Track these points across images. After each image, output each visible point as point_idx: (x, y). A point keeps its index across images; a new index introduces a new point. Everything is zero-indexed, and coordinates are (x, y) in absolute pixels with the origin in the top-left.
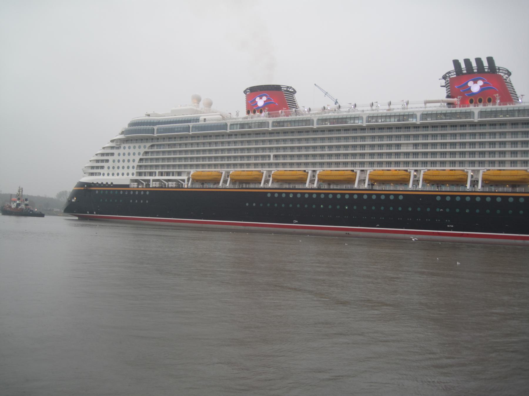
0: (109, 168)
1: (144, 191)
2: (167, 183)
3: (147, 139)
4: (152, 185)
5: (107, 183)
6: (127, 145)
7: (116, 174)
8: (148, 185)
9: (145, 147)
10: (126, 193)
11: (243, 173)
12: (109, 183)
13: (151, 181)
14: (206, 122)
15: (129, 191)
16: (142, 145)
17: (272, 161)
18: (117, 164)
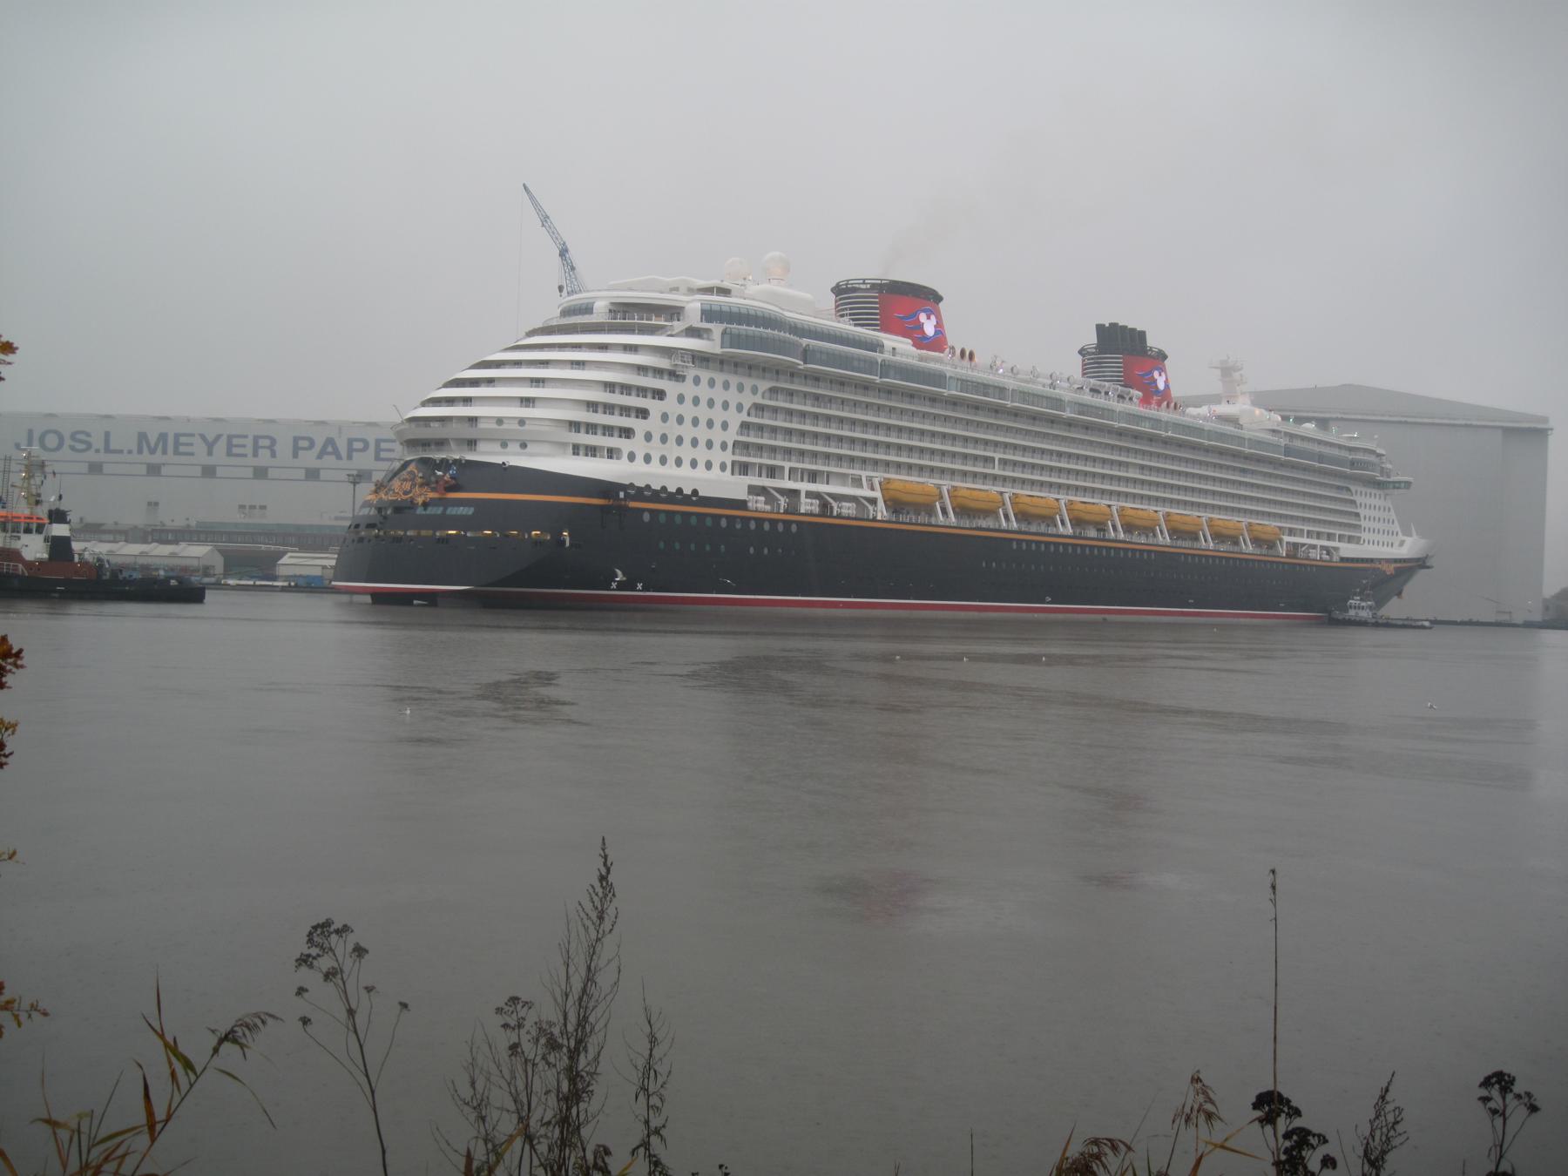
0: (648, 437)
1: (784, 522)
2: (835, 505)
3: (764, 369)
4: (806, 505)
5: (680, 490)
6: (705, 375)
7: (671, 461)
8: (792, 509)
9: (754, 390)
10: (738, 526)
11: (975, 493)
12: (687, 491)
13: (803, 495)
14: (898, 358)
15: (746, 520)
16: (748, 383)
17: (997, 471)
18: (673, 430)
